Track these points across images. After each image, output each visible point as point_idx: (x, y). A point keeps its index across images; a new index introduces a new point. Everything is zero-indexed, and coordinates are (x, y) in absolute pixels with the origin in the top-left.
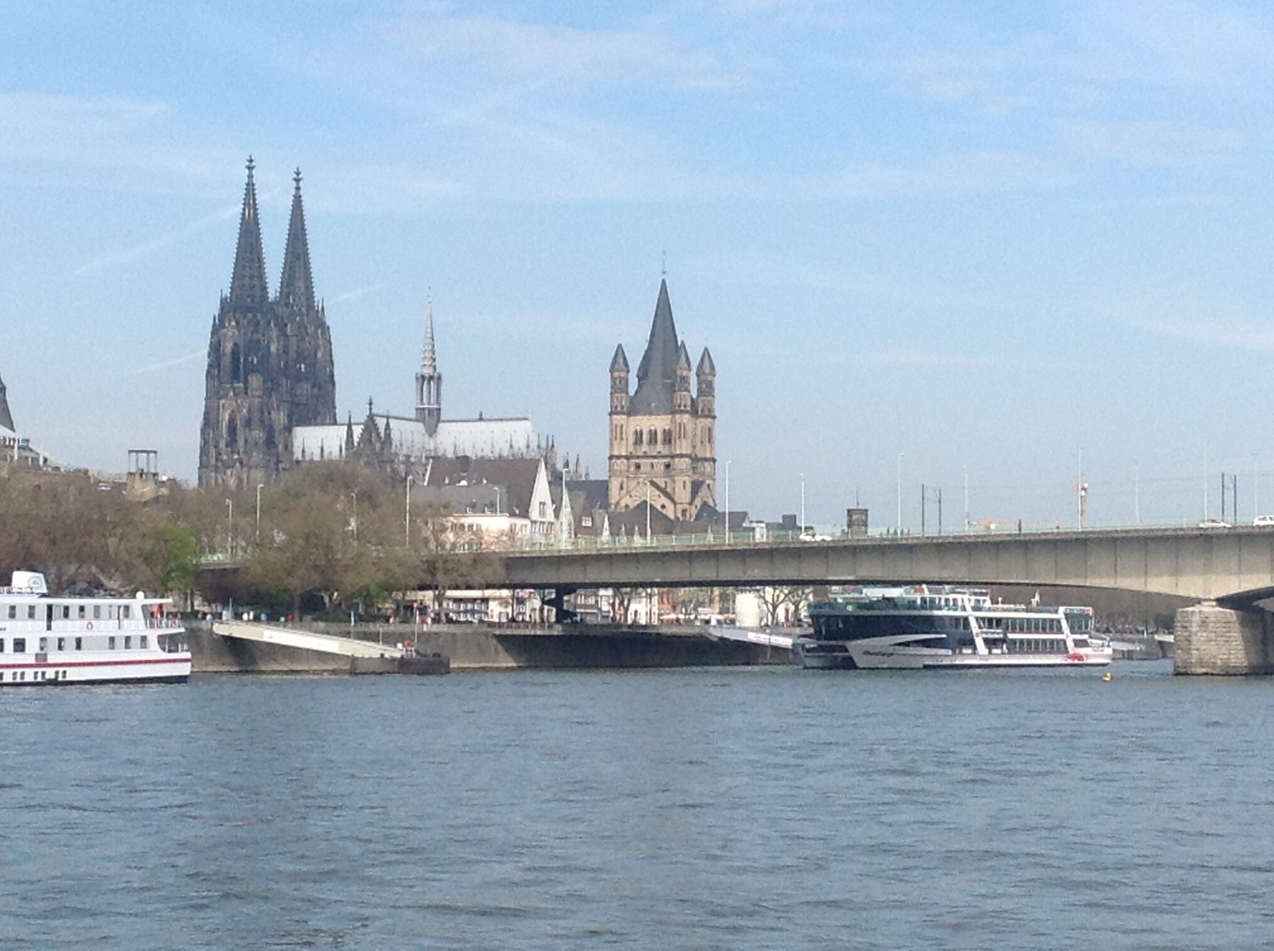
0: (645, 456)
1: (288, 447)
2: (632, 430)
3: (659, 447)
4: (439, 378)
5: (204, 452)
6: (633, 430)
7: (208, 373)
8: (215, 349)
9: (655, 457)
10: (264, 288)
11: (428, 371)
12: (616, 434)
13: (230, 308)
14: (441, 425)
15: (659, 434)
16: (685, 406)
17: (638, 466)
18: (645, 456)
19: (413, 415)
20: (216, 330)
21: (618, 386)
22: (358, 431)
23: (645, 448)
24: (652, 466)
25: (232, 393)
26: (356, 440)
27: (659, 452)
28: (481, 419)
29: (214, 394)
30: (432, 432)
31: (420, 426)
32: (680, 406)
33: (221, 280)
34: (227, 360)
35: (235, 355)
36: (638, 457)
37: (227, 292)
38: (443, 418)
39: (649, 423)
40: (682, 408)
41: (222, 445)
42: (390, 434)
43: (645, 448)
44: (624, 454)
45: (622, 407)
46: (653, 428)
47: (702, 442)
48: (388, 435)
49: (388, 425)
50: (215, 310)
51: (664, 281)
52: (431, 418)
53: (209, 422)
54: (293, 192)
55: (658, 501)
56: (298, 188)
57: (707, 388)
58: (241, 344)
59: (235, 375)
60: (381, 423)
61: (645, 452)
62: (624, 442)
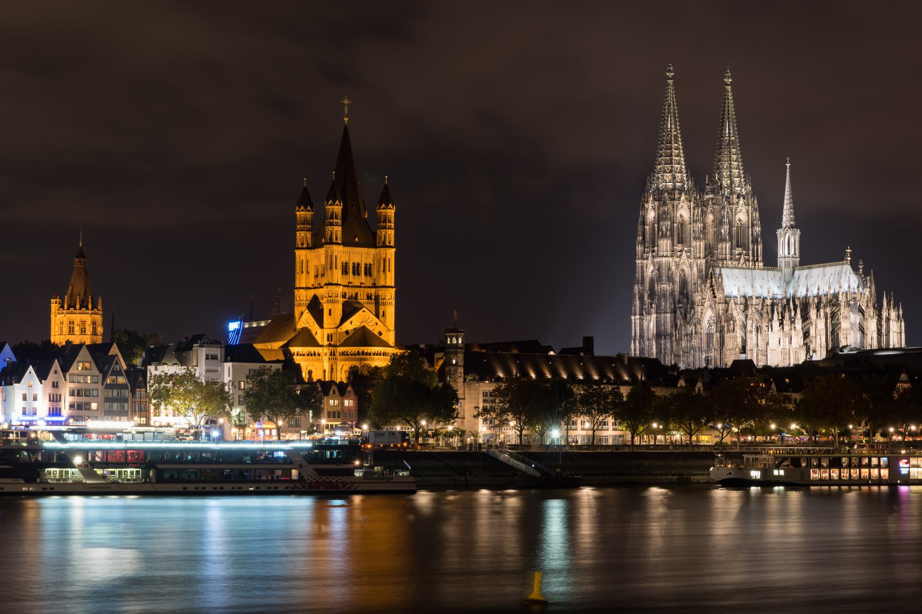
27: (319, 284)
41: (646, 298)
44: (304, 286)
45: (308, 244)
49: (720, 275)
51: (346, 127)
62: (304, 275)
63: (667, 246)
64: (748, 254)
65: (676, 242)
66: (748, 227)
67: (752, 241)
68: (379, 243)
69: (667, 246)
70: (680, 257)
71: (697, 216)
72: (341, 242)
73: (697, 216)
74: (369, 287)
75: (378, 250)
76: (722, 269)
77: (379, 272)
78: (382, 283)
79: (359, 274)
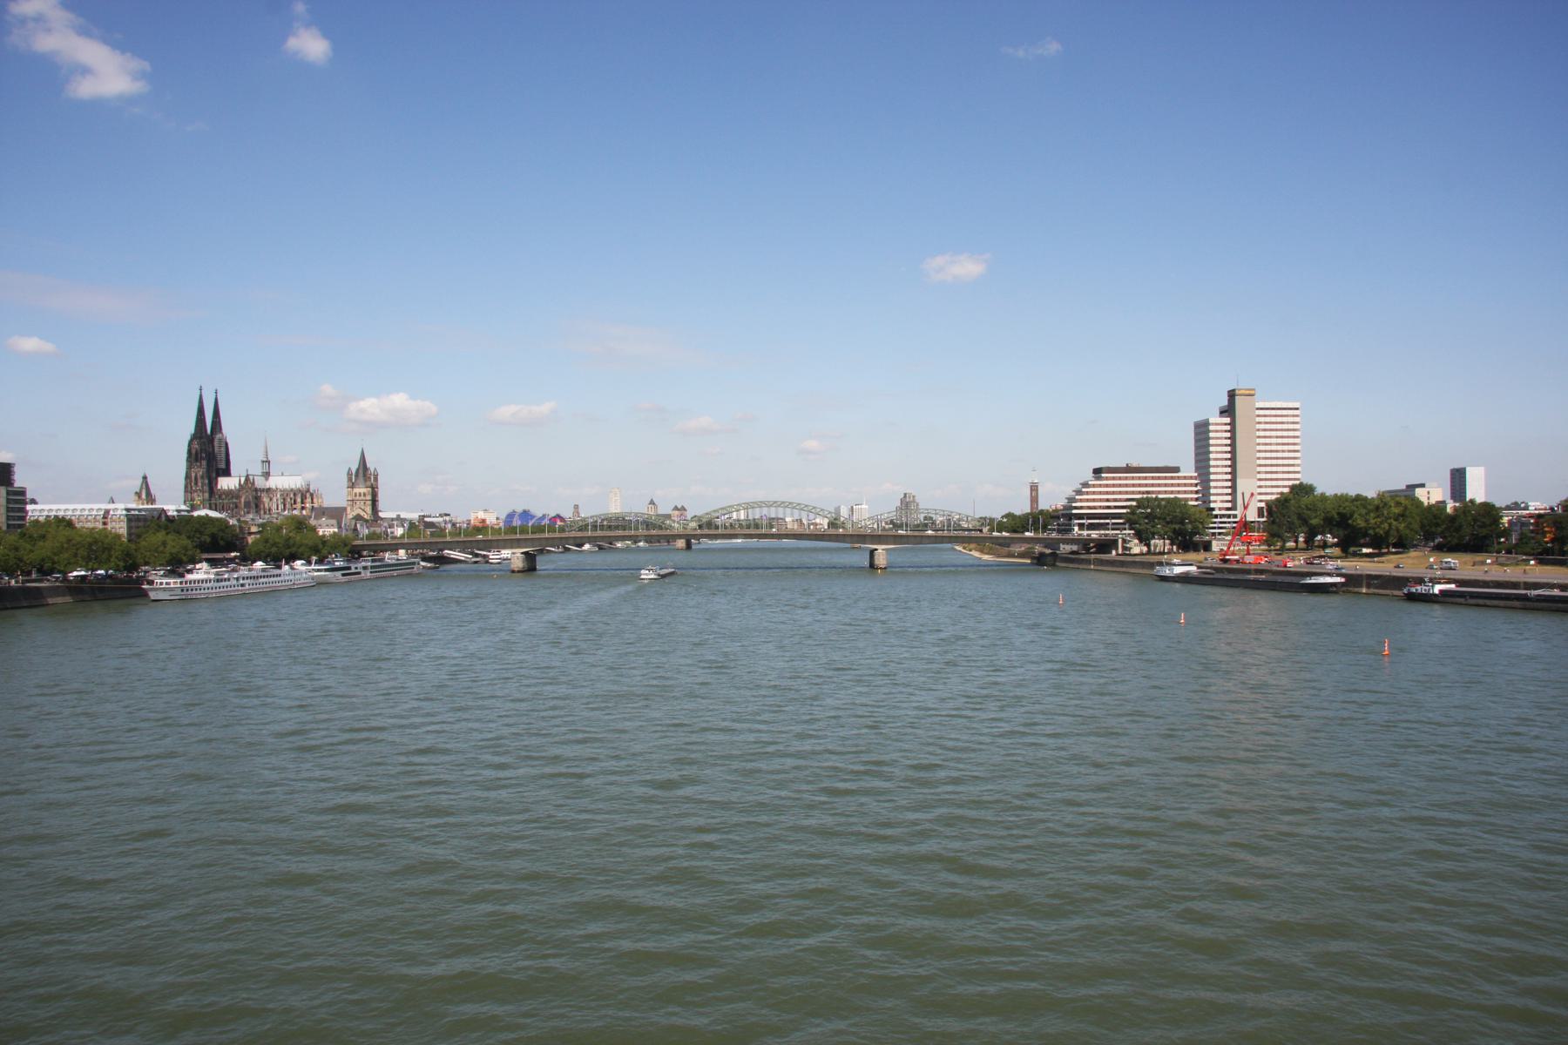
1: (216, 484)
3: (362, 498)
5: (186, 487)
7: (187, 460)
8: (189, 452)
10: (206, 431)
11: (265, 459)
12: (349, 494)
13: (194, 438)
20: (189, 445)
21: (350, 479)
22: (243, 480)
23: (358, 498)
26: (242, 482)
28: (282, 475)
29: (189, 467)
30: (267, 479)
31: (263, 478)
33: (190, 428)
34: (193, 456)
35: (196, 453)
37: (193, 432)
43: (358, 498)
49: (253, 479)
50: (189, 438)
52: (267, 475)
53: (188, 477)
54: (214, 397)
55: (362, 513)
57: (376, 479)
58: (199, 450)
59: (196, 460)
60: (251, 478)
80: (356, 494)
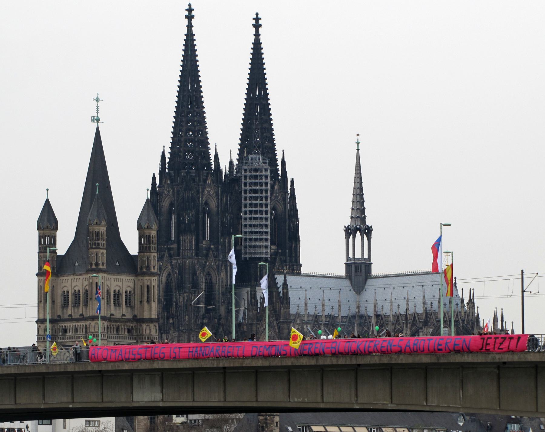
0: (71, 319)
2: (59, 292)
4: (367, 232)
6: (61, 292)
9: (77, 320)
14: (370, 282)
15: (70, 294)
16: (103, 264)
17: (65, 331)
18: (71, 319)
19: (342, 271)
23: (70, 311)
24: (76, 330)
25: (167, 255)
32: (91, 265)
36: (65, 320)
38: (375, 272)
39: (73, 285)
40: (94, 267)
42: (287, 292)
46: (77, 289)
47: (141, 302)
48: (286, 294)
49: (285, 284)
54: (253, 39)
56: (257, 35)
61: (71, 315)
63: (191, 242)
64: (284, 254)
65: (201, 237)
66: (286, 221)
67: (289, 238)
68: (141, 268)
69: (191, 242)
70: (207, 256)
71: (226, 204)
72: (105, 267)
73: (226, 204)
74: (128, 320)
75: (140, 278)
76: (288, 277)
77: (141, 302)
78: (146, 316)
79: (119, 305)
80: (65, 296)
